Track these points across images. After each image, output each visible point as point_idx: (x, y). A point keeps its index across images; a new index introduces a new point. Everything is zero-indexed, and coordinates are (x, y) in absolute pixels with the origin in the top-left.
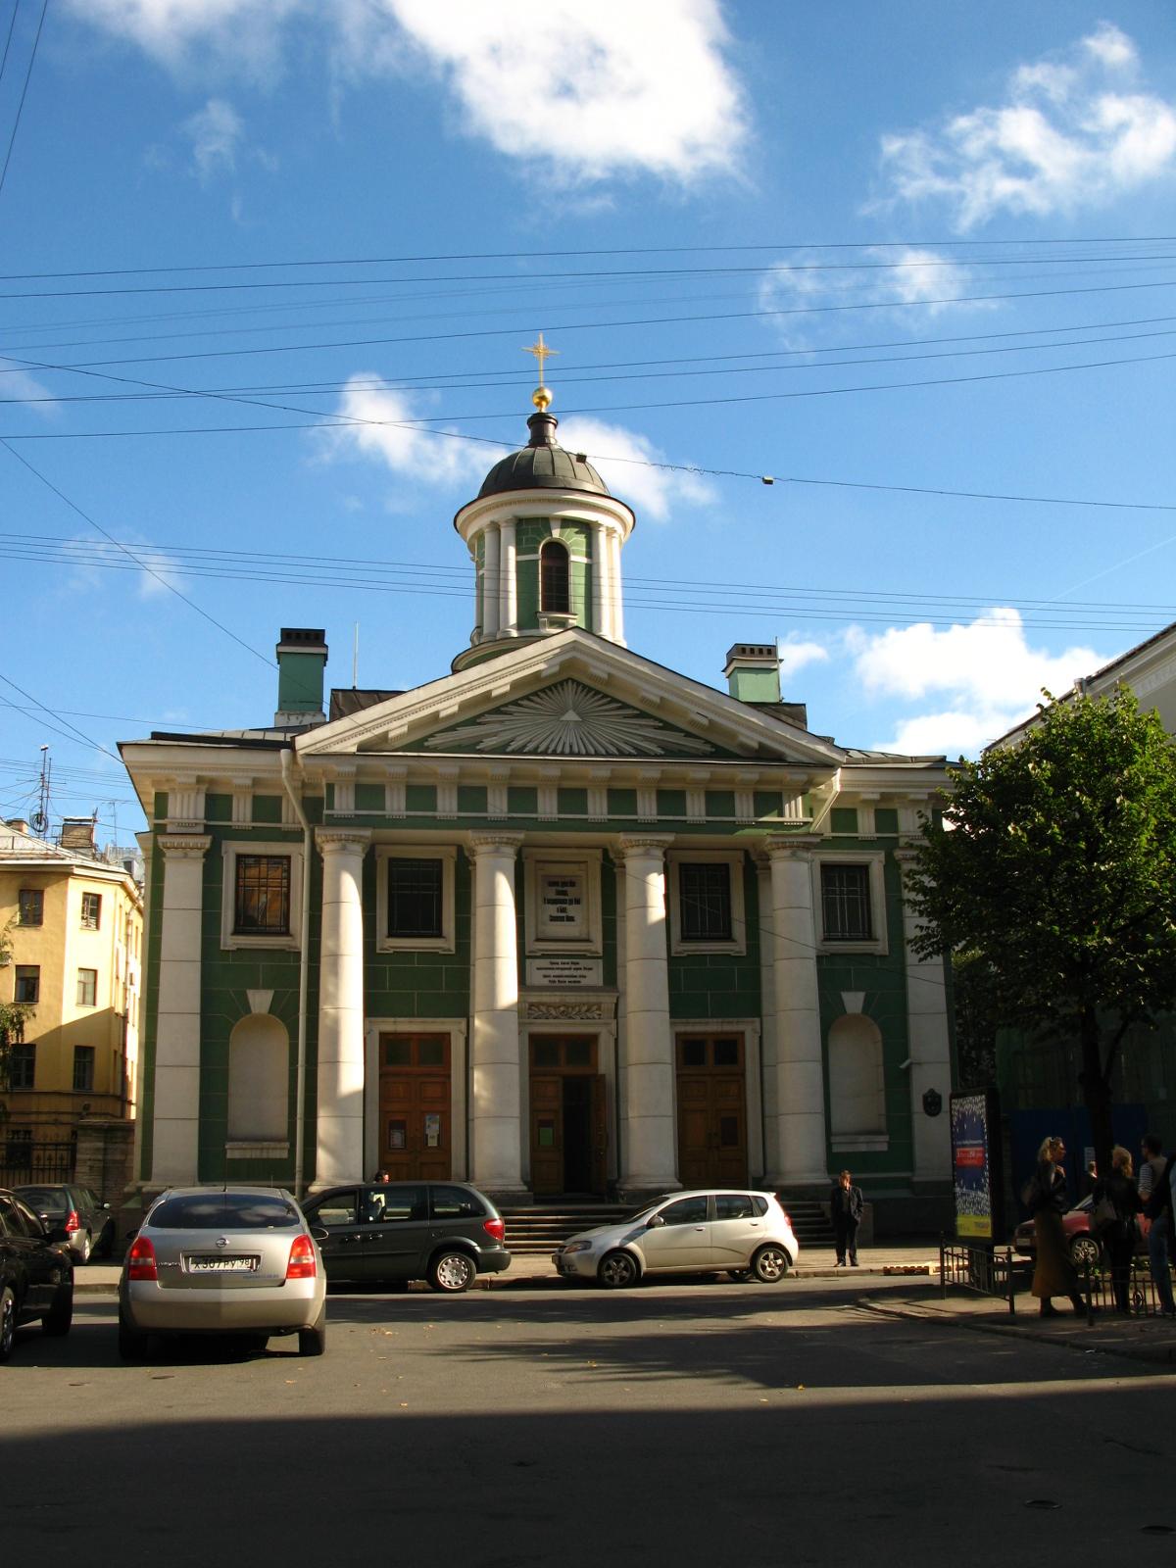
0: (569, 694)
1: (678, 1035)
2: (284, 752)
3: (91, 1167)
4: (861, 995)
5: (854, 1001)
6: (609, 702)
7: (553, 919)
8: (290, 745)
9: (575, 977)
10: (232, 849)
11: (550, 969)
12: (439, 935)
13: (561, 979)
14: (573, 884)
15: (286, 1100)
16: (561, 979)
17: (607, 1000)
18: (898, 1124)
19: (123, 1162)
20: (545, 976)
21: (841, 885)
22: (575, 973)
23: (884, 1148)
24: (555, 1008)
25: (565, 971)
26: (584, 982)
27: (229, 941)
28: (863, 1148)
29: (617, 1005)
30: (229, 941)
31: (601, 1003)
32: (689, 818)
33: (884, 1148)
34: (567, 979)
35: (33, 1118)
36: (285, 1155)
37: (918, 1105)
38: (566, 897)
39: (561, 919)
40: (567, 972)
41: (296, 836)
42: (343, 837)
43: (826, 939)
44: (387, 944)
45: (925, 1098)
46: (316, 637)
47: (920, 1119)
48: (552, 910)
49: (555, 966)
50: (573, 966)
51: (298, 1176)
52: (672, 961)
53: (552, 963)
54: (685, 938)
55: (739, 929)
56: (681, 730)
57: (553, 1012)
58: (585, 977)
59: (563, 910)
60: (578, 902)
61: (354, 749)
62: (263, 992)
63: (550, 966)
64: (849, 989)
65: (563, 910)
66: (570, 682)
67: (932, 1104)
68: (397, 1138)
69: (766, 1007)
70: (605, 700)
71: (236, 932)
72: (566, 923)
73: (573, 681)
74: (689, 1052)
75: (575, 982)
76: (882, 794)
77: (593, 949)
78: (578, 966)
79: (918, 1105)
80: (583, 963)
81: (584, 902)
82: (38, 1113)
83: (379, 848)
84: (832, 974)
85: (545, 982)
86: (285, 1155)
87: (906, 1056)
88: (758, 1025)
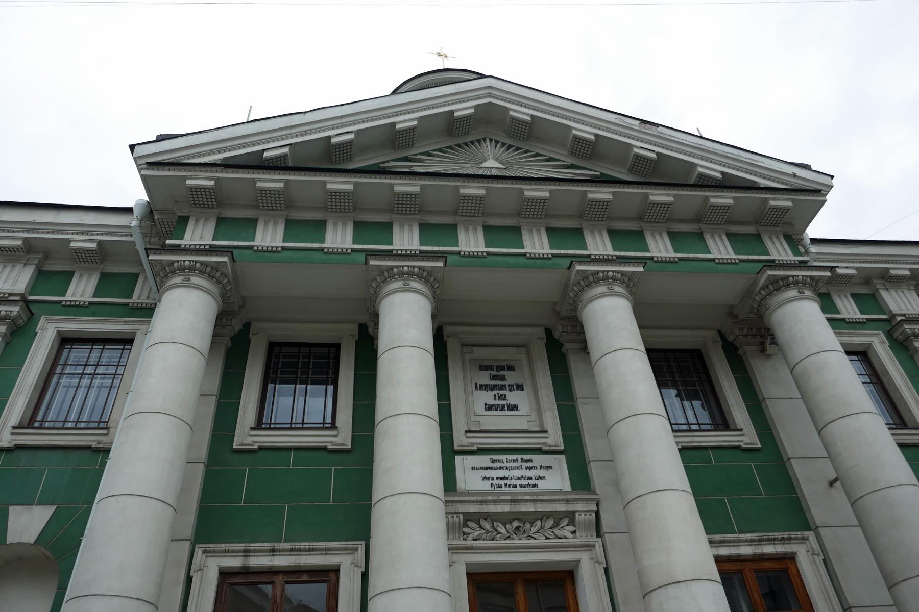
7: (489, 408)
9: (529, 478)
11: (491, 468)
13: (509, 482)
14: (511, 368)
16: (509, 482)
17: (582, 508)
20: (484, 479)
22: (528, 473)
24: (505, 525)
26: (543, 485)
29: (597, 513)
31: (573, 513)
34: (518, 483)
38: (504, 383)
39: (502, 408)
42: (187, 263)
48: (488, 397)
49: (498, 465)
50: (524, 464)
53: (493, 461)
57: (502, 529)
58: (543, 478)
60: (520, 387)
63: (492, 465)
65: (502, 397)
66: (488, 140)
72: (507, 413)
75: (528, 486)
77: (550, 441)
78: (530, 464)
80: (538, 460)
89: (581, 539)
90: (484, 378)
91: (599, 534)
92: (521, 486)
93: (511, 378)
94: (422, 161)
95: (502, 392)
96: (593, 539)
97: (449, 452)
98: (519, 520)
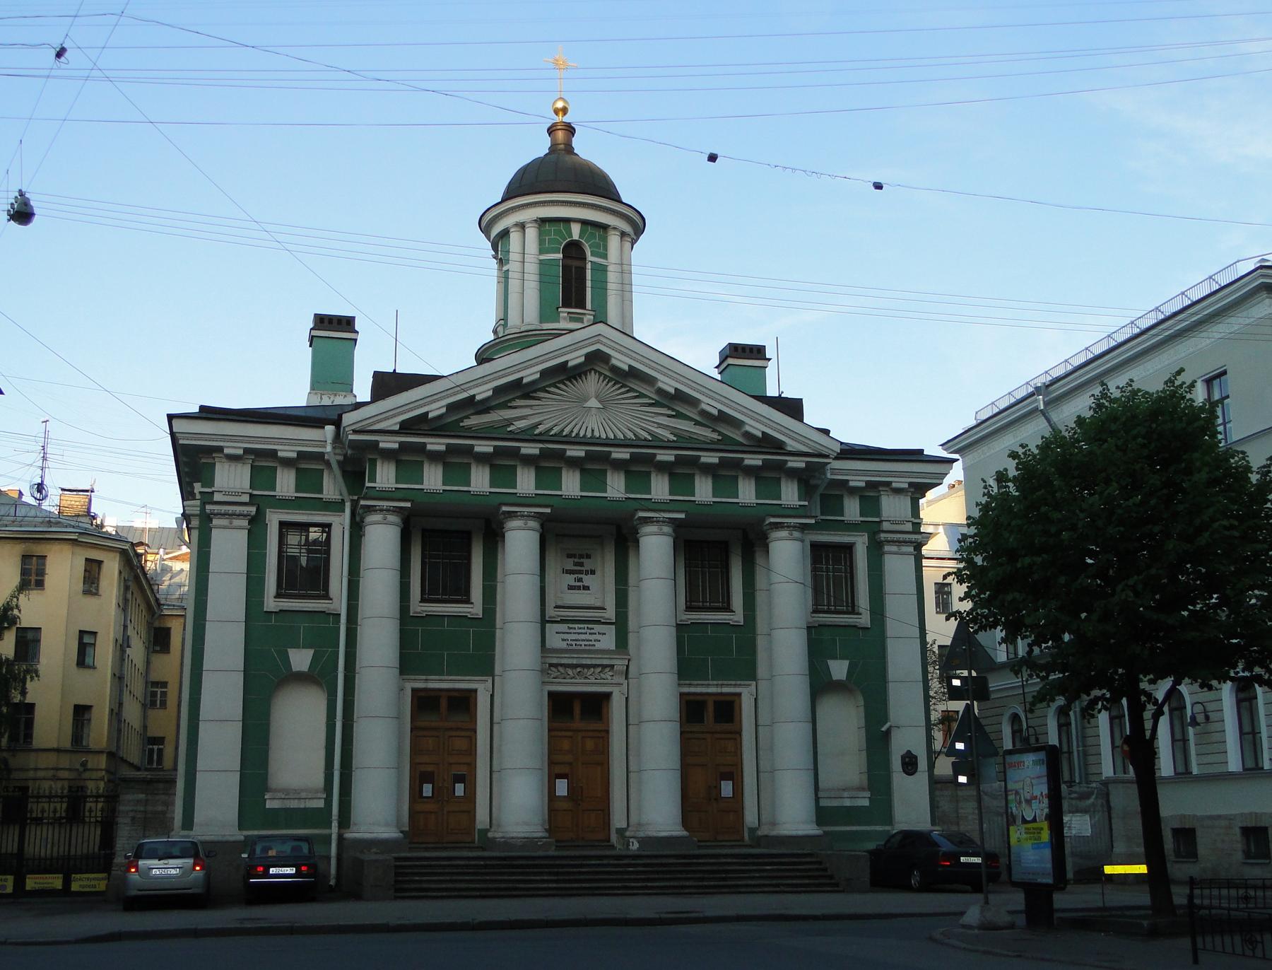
0: (592, 384)
1: (682, 695)
2: (330, 429)
3: (133, 818)
4: (846, 663)
5: (839, 669)
6: (627, 392)
7: (571, 588)
8: (337, 423)
10: (273, 519)
12: (468, 601)
14: (589, 557)
15: (322, 753)
17: (619, 663)
18: (878, 781)
19: (164, 813)
21: (827, 563)
23: (866, 803)
25: (580, 635)
26: (598, 646)
27: (271, 603)
28: (847, 803)
30: (271, 603)
32: (697, 498)
33: (866, 803)
35: (31, 774)
36: (321, 804)
37: (896, 764)
39: (579, 588)
40: (583, 637)
41: (337, 506)
43: (814, 612)
44: (418, 607)
45: (903, 757)
46: (347, 323)
47: (899, 777)
48: (570, 580)
51: (335, 824)
52: (680, 627)
54: (689, 608)
55: (863, 601)
56: (691, 419)
59: (580, 580)
60: (593, 572)
61: (397, 428)
62: (305, 651)
64: (835, 658)
65: (580, 580)
67: (910, 764)
68: (427, 790)
69: (762, 670)
70: (623, 390)
71: (278, 596)
74: (691, 709)
76: (867, 482)
79: (896, 764)
80: (597, 628)
81: (598, 573)
82: (36, 769)
84: (819, 644)
85: (563, 645)
86: (321, 804)
87: (885, 718)
88: (753, 687)
89: (616, 680)
90: (569, 564)
91: (627, 678)
93: (588, 564)
94: (539, 399)
96: (622, 680)
97: (544, 621)
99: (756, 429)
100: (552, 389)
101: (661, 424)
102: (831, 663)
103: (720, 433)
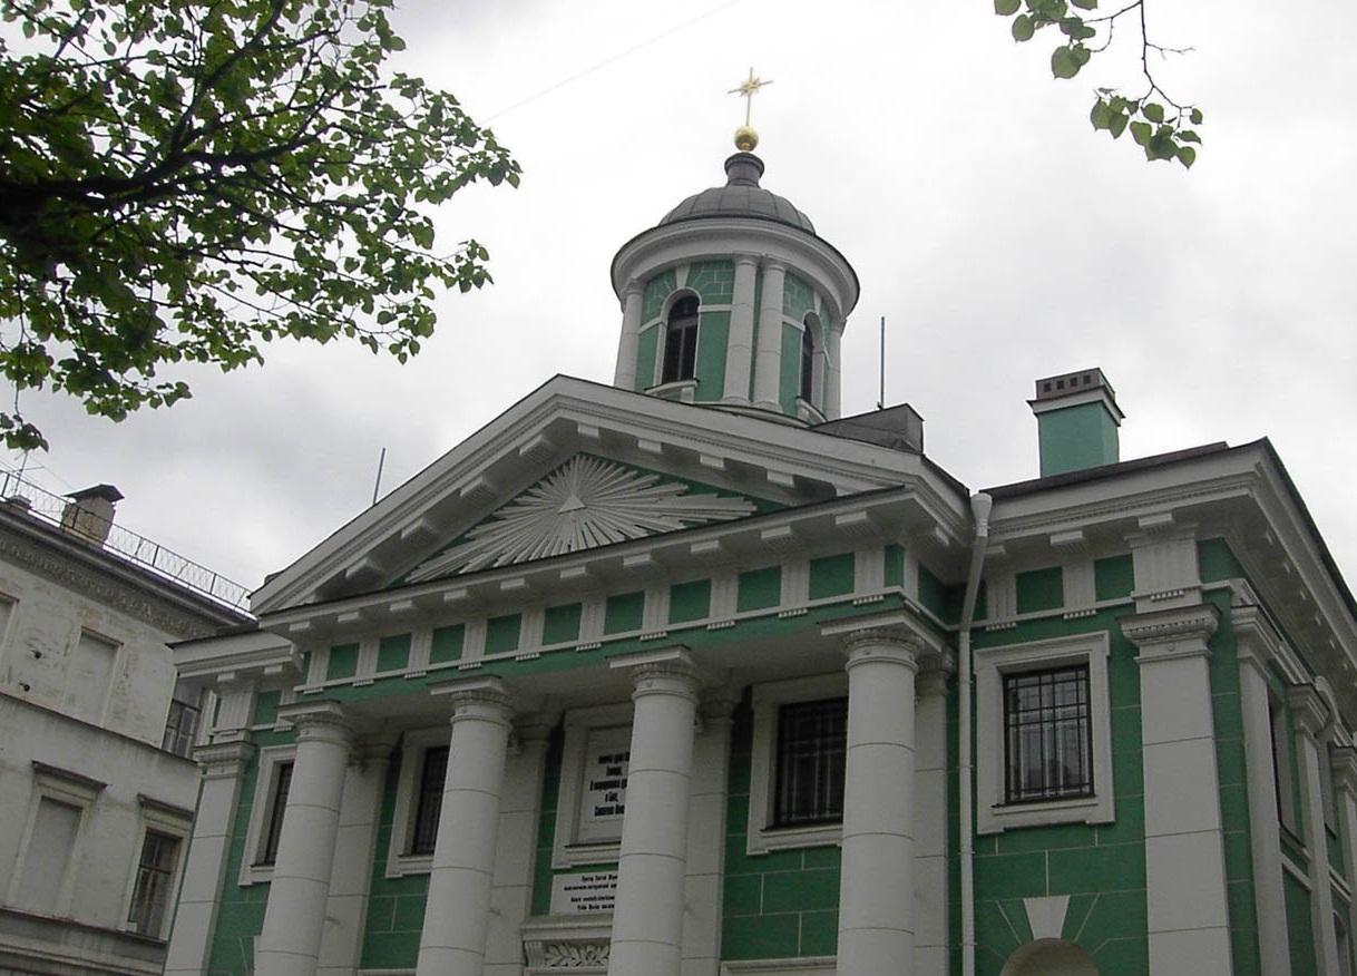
6: (625, 472)
7: (600, 812)
13: (593, 903)
16: (593, 903)
20: (573, 900)
34: (600, 903)
49: (589, 883)
53: (585, 879)
59: (613, 797)
63: (583, 884)
73: (582, 454)
83: (409, 735)
85: (573, 909)
92: (604, 907)
95: (614, 790)
98: (592, 944)
99: (781, 474)
100: (524, 499)
101: (665, 510)
102: (1030, 904)
103: (755, 501)
